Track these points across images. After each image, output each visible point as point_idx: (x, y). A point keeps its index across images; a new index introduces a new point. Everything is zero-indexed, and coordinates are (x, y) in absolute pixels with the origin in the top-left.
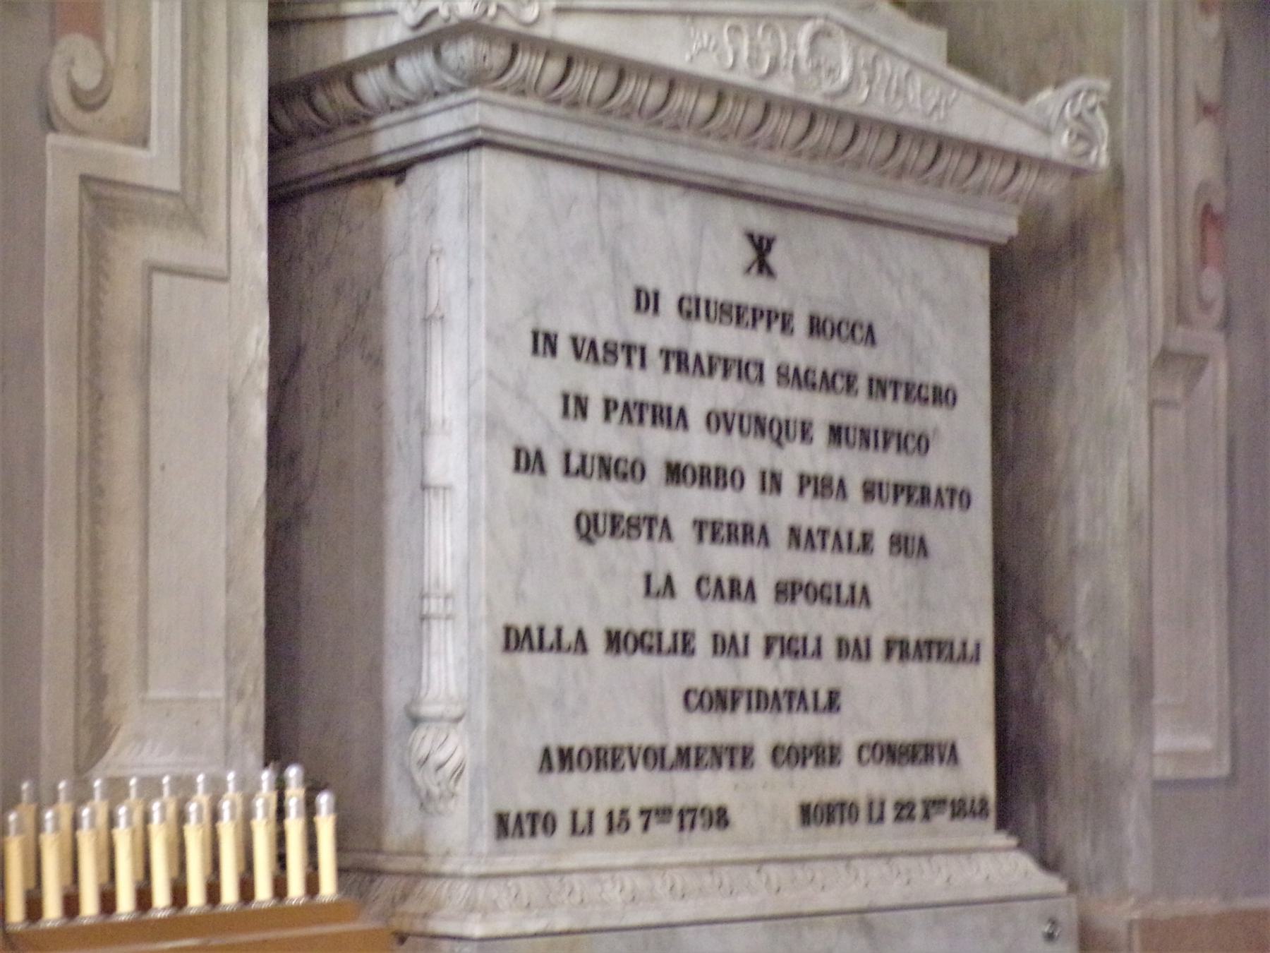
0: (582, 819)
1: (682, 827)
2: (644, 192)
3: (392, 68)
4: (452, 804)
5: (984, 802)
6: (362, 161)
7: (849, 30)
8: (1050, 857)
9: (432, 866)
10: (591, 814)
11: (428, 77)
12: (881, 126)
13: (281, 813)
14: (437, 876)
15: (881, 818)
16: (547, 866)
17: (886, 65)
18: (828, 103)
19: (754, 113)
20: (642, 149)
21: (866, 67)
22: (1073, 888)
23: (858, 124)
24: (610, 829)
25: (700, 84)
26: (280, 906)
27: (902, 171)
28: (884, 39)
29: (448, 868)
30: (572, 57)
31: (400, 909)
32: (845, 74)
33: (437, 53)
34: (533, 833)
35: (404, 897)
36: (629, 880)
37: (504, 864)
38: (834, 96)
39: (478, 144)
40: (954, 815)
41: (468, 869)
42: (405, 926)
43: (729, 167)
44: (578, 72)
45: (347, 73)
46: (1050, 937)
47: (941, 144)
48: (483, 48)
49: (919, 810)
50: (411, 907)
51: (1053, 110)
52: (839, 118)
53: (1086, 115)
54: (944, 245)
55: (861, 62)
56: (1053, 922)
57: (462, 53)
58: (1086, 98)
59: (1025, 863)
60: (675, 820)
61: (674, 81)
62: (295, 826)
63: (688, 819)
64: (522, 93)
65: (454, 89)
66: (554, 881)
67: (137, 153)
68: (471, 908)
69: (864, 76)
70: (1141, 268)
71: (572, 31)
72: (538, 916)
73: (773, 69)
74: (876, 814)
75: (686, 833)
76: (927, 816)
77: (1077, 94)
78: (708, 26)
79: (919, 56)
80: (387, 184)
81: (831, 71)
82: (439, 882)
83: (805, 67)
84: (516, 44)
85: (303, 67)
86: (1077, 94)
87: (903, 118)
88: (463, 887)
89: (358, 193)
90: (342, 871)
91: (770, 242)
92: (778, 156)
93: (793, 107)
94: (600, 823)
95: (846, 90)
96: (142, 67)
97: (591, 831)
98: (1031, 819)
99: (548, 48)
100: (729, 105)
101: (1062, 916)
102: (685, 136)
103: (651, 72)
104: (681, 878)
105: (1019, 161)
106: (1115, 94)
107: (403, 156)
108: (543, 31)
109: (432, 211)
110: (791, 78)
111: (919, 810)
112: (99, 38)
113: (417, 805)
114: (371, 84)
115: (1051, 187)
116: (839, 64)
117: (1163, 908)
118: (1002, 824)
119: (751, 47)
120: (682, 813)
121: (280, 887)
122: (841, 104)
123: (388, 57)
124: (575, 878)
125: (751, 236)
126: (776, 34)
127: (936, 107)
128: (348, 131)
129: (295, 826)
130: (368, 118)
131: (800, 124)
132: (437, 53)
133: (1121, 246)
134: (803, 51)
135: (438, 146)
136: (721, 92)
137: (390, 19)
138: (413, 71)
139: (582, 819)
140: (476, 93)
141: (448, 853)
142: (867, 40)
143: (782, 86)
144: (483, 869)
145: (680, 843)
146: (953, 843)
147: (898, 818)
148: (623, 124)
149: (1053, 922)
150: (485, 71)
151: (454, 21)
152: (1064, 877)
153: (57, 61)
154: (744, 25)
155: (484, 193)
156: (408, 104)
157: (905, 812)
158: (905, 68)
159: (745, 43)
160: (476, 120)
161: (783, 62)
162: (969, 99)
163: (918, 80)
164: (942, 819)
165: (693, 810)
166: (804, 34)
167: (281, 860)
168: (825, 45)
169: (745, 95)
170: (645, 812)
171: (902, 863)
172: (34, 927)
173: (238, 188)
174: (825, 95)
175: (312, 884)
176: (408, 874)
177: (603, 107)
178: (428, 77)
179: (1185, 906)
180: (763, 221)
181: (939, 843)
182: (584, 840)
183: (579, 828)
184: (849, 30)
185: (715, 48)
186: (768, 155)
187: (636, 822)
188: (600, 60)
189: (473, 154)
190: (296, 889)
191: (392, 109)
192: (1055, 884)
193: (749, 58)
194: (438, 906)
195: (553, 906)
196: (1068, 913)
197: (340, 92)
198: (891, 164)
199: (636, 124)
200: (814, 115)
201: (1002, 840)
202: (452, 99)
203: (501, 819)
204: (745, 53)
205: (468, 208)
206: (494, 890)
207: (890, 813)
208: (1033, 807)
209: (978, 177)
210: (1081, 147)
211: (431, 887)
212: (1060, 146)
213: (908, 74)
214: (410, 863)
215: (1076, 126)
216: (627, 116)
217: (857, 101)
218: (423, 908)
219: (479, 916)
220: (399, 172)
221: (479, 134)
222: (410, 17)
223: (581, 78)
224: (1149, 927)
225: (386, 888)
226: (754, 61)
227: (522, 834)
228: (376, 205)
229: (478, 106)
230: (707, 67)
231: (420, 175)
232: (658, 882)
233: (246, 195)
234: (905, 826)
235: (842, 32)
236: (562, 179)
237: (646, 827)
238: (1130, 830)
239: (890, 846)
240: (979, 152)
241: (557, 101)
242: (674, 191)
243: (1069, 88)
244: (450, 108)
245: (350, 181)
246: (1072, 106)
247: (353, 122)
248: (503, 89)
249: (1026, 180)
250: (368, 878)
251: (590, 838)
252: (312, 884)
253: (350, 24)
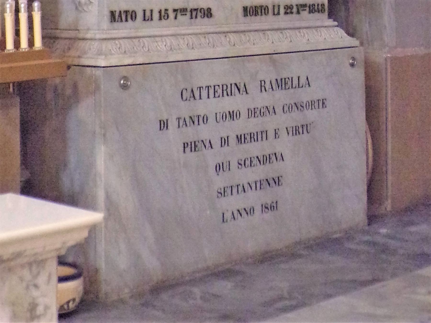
0: (148, 14)
1: (192, 18)
4: (90, 7)
5: (323, 5)
8: (351, 31)
9: (81, 36)
10: (152, 11)
13: (17, 11)
14: (84, 39)
15: (279, 14)
16: (133, 35)
22: (362, 44)
24: (160, 19)
26: (32, 50)
29: (88, 36)
31: (67, 54)
34: (126, 20)
35: (69, 49)
36: (168, 41)
37: (115, 34)
40: (310, 12)
41: (98, 36)
42: (70, 62)
46: (352, 65)
49: (295, 10)
50: (73, 53)
56: (353, 59)
59: (341, 32)
60: (189, 14)
62: (23, 17)
63: (194, 13)
66: (136, 41)
68: (100, 53)
72: (130, 57)
74: (276, 12)
75: (193, 20)
76: (298, 12)
82: (86, 41)
88: (96, 44)
90: (43, 38)
94: (156, 16)
97: (152, 19)
98: (343, 14)
101: (357, 56)
104: (192, 40)
111: (295, 10)
113: (74, 8)
117: (399, 52)
118: (330, 16)
120: (191, 11)
121: (17, 44)
124: (144, 40)
129: (23, 17)
139: (148, 14)
141: (88, 29)
144: (104, 36)
145: (191, 25)
146: (311, 24)
147: (286, 13)
149: (353, 59)
152: (357, 39)
157: (289, 11)
164: (305, 14)
165: (196, 10)
167: (17, 33)
170: (175, 10)
171: (288, 33)
175: (31, 43)
176: (70, 39)
179: (409, 51)
181: (304, 24)
182: (148, 23)
183: (147, 18)
187: (172, 15)
190: (24, 44)
192: (354, 42)
194: (85, 53)
195: (136, 53)
196: (359, 54)
201: (331, 22)
203: (112, 14)
206: (109, 45)
207: (282, 11)
208: (343, 8)
211: (81, 44)
214: (72, 34)
218: (78, 54)
219: (103, 57)
224: (395, 60)
225: (60, 45)
227: (122, 21)
232: (182, 41)
234: (289, 16)
237: (176, 18)
238: (386, 18)
239: (283, 25)
250: (52, 41)
251: (152, 22)
252: (31, 43)
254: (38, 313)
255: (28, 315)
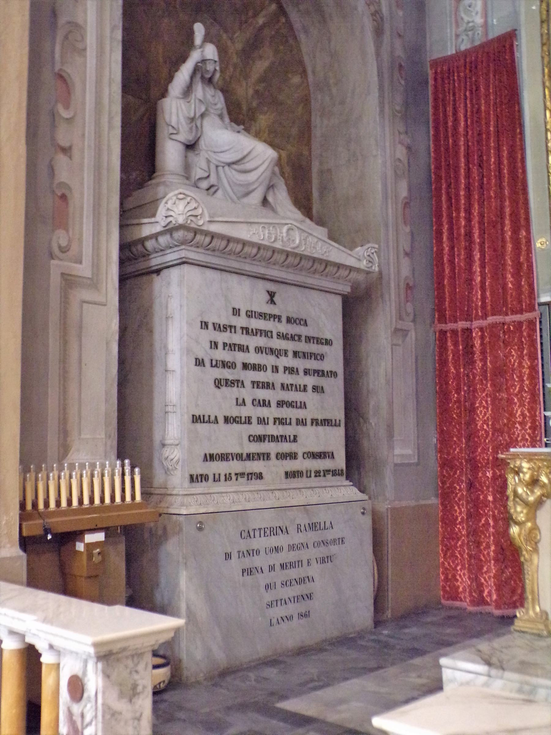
0: (217, 476)
1: (248, 480)
2: (235, 277)
3: (157, 239)
4: (175, 472)
5: (342, 470)
6: (147, 268)
7: (298, 228)
8: (362, 489)
9: (169, 492)
10: (219, 474)
11: (168, 241)
12: (308, 258)
13: (123, 474)
14: (171, 495)
15: (310, 476)
16: (206, 492)
17: (310, 239)
18: (292, 250)
19: (269, 253)
20: (235, 265)
21: (304, 239)
22: (370, 498)
23: (302, 257)
24: (226, 480)
25: (252, 244)
27: (315, 272)
28: (310, 231)
29: (174, 492)
30: (213, 236)
31: (159, 506)
32: (297, 242)
33: (171, 235)
34: (202, 481)
35: (160, 502)
36: (231, 496)
37: (193, 491)
38: (294, 248)
39: (184, 263)
40: (333, 475)
41: (181, 493)
42: (161, 511)
43: (262, 271)
44: (215, 241)
45: (142, 241)
46: (363, 513)
47: (327, 263)
48: (186, 233)
49: (322, 474)
50: (163, 505)
51: (361, 254)
52: (296, 255)
53: (371, 256)
54: (328, 295)
55: (302, 238)
56: (364, 509)
57: (179, 235)
58: (371, 250)
59: (355, 490)
60: (246, 477)
61: (244, 243)
62: (128, 478)
63: (250, 476)
64: (198, 247)
65: (176, 246)
66: (208, 496)
67: (78, 266)
68: (182, 505)
69: (303, 243)
70: (388, 303)
71: (214, 228)
72: (204, 507)
73: (275, 241)
74: (308, 475)
75: (249, 481)
76: (324, 476)
77: (368, 248)
78: (256, 226)
79: (320, 237)
80: (154, 276)
81: (293, 240)
82: (172, 497)
83: (285, 239)
84: (196, 232)
85: (129, 239)
86: (368, 248)
87: (316, 255)
88: (179, 499)
89: (145, 278)
90: (142, 494)
91: (274, 293)
92: (277, 267)
93: (281, 251)
94: (223, 478)
95: (297, 247)
96: (80, 240)
97: (220, 481)
98: (356, 477)
99: (206, 233)
100: (262, 251)
101: (367, 507)
102: (248, 260)
103: (238, 241)
104: (248, 495)
105: (351, 269)
106: (379, 249)
107: (159, 267)
108: (205, 228)
109: (169, 283)
110: (281, 243)
111: (322, 474)
112: (67, 231)
114: (150, 245)
115: (361, 277)
116: (295, 238)
117: (397, 504)
118: (347, 478)
119: (269, 233)
120: (248, 475)
121: (123, 498)
122: (296, 251)
123: (155, 236)
124: (215, 496)
125: (268, 292)
126: (276, 229)
127: (326, 252)
128: (142, 259)
129: (128, 478)
130: (149, 255)
131: (283, 257)
132: (171, 235)
133: (382, 296)
134: (285, 235)
135: (171, 263)
136: (259, 247)
137: (156, 224)
138: (163, 240)
139: (217, 476)
140: (183, 247)
141: (174, 488)
142: (304, 231)
143: (278, 245)
144: (186, 493)
145: (248, 484)
146: (334, 484)
147: (316, 476)
148: (228, 257)
149: (364, 509)
150: (186, 240)
151: (177, 225)
152: (367, 495)
153: (55, 238)
154: (266, 226)
155: (185, 278)
156: (162, 250)
157: (318, 474)
158: (316, 240)
159: (267, 232)
160: (183, 256)
161: (279, 238)
162: (336, 249)
163: (320, 244)
164: (329, 477)
165: (251, 474)
166: (285, 229)
167: (123, 490)
168: (291, 232)
169: (266, 248)
170: (236, 474)
171: (317, 490)
172: (47, 510)
173: (109, 276)
174: (292, 248)
175: (133, 497)
176: (161, 494)
177: (223, 251)
178: (168, 241)
179: (404, 503)
180: (272, 287)
181: (328, 484)
182: (217, 483)
183: (216, 480)
184: (298, 228)
185: (258, 233)
186: (274, 267)
187: (234, 477)
188: (222, 237)
189: (182, 266)
190: (128, 498)
191: (157, 252)
192: (364, 497)
193: (268, 237)
194: (172, 505)
195: (208, 504)
196: (368, 506)
197: (140, 247)
198: (312, 269)
199: (233, 257)
200: (288, 254)
201: (348, 483)
202: (175, 249)
203: (191, 476)
204: (267, 235)
205: (180, 284)
206: (189, 499)
207: (313, 474)
208: (356, 472)
209: (337, 275)
210: (370, 265)
211: (169, 498)
212: (363, 265)
213: (317, 242)
214: (162, 491)
215: (368, 258)
216: (230, 254)
217: (301, 250)
218: (167, 505)
219: (185, 507)
220: (158, 272)
221: (184, 260)
222: (163, 224)
223: (216, 243)
224: (393, 509)
225: (154, 499)
226: (269, 238)
227: (198, 482)
228: (151, 282)
229: (184, 251)
230: (255, 239)
231: (165, 273)
232: (241, 496)
233: (112, 279)
234: (318, 478)
235: (296, 229)
236: (209, 273)
237: (237, 480)
238: (387, 480)
239: (314, 485)
240: (339, 266)
241: (208, 250)
242: (244, 278)
243: (366, 247)
244: (174, 252)
245: (143, 274)
246: (367, 252)
247: (144, 256)
248: (192, 246)
249: (353, 275)
250: (148, 496)
251: (220, 482)
252: (133, 497)
253: (143, 226)
254: (138, 691)
255: (131, 692)
